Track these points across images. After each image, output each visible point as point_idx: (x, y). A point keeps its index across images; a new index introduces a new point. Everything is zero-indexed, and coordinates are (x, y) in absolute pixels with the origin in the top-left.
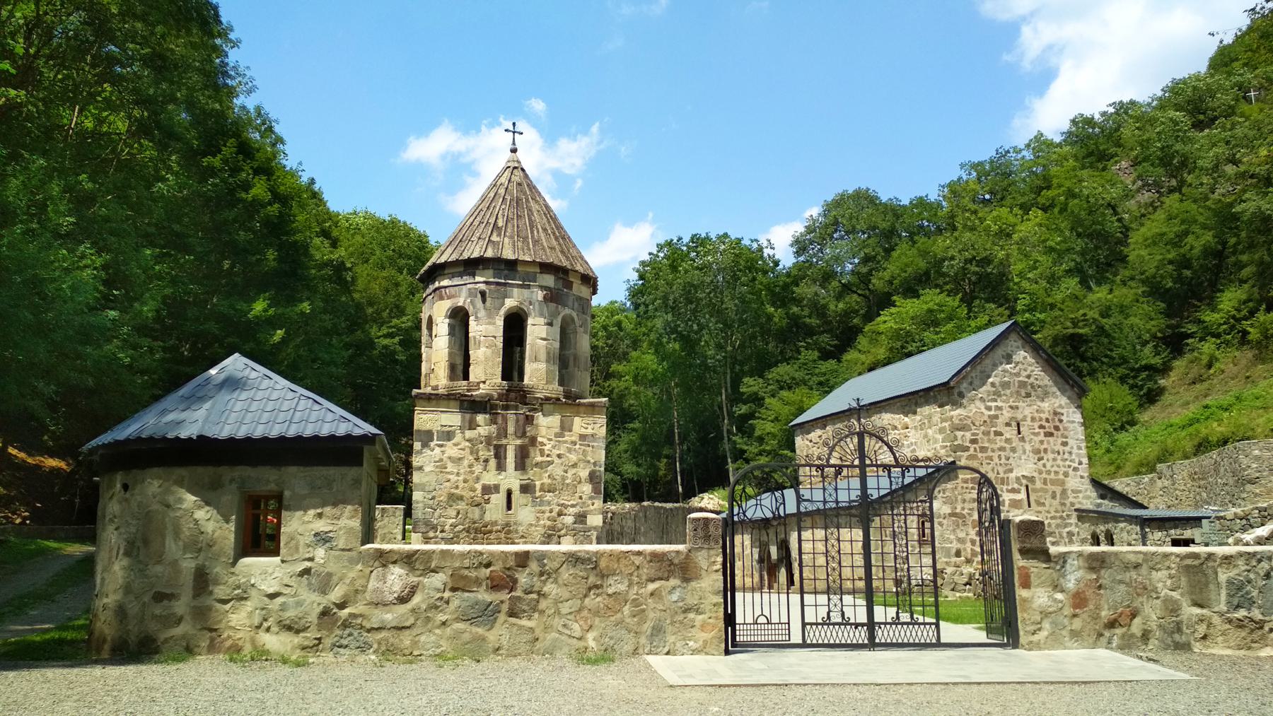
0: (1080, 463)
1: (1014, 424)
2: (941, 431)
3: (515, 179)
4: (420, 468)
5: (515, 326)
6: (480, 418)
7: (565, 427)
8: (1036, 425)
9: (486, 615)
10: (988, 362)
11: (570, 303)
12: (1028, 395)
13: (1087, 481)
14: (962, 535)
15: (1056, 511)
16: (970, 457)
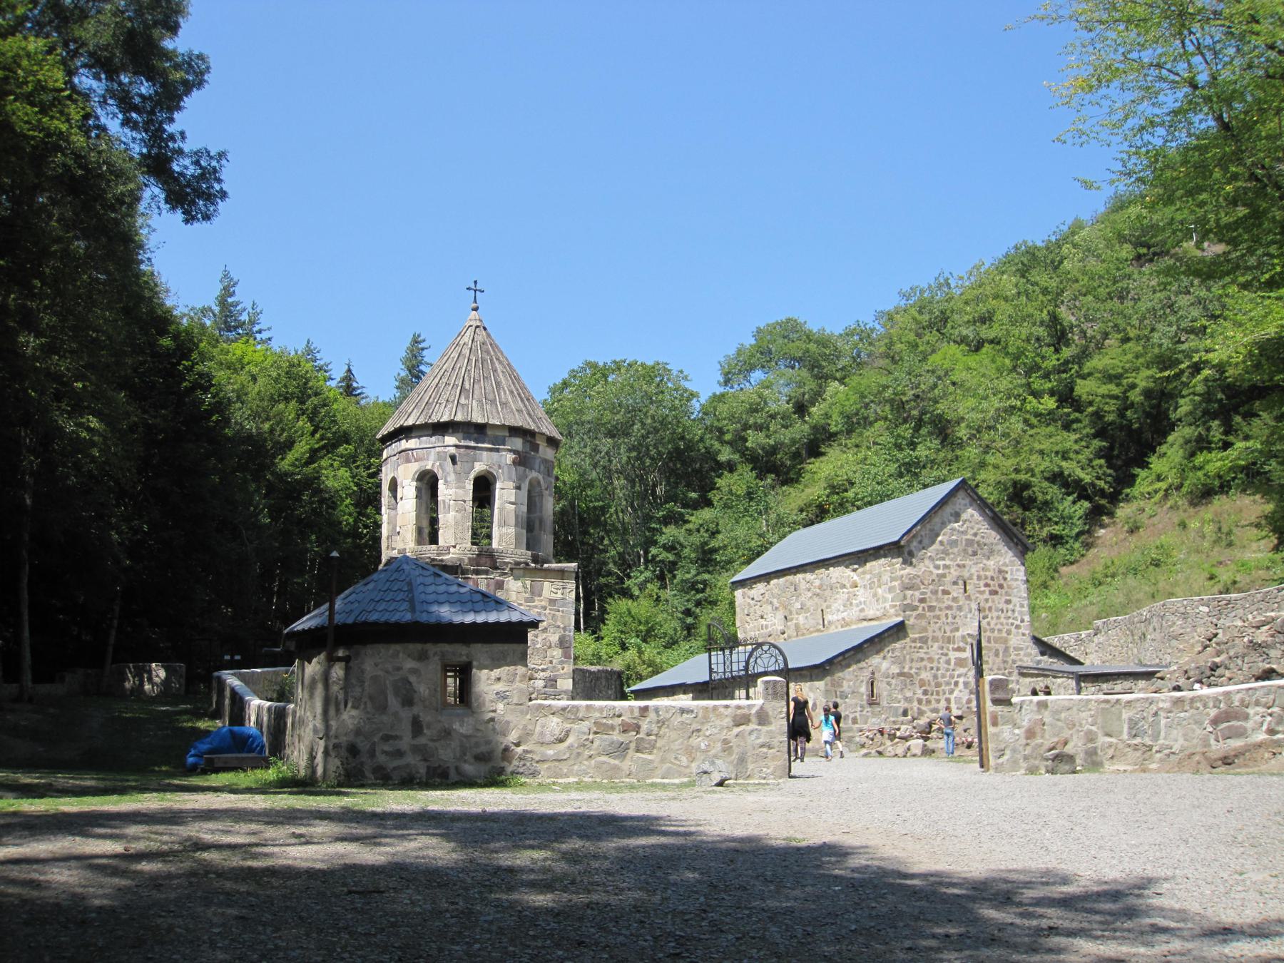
0: (1022, 621)
1: (961, 582)
2: (891, 590)
3: (479, 338)
5: (483, 489)
8: (982, 583)
9: (620, 750)
10: (937, 520)
11: (537, 467)
12: (975, 554)
13: (1028, 638)
14: (909, 694)
15: (999, 669)
16: (919, 617)
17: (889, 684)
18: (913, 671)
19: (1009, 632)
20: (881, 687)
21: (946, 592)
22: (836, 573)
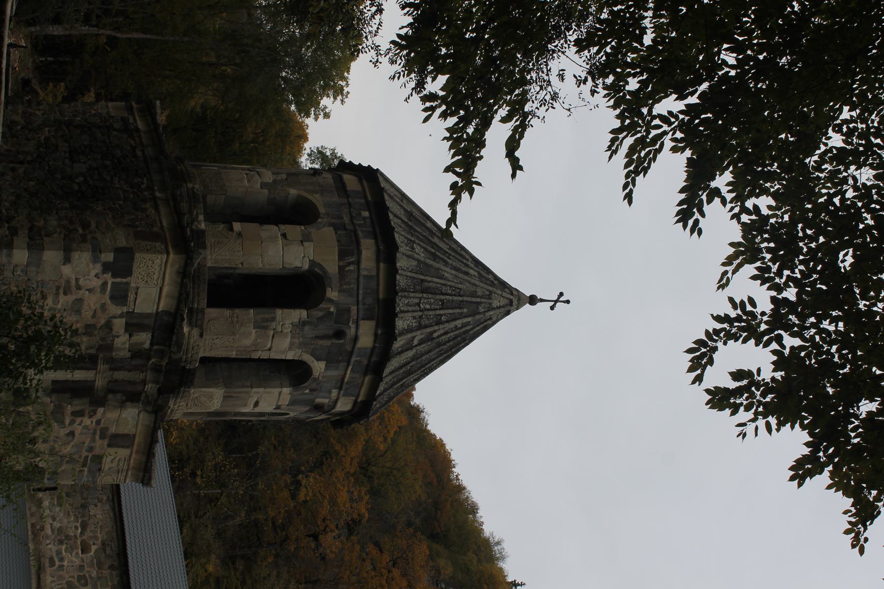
4: (67, 260)
6: (144, 338)
7: (118, 440)
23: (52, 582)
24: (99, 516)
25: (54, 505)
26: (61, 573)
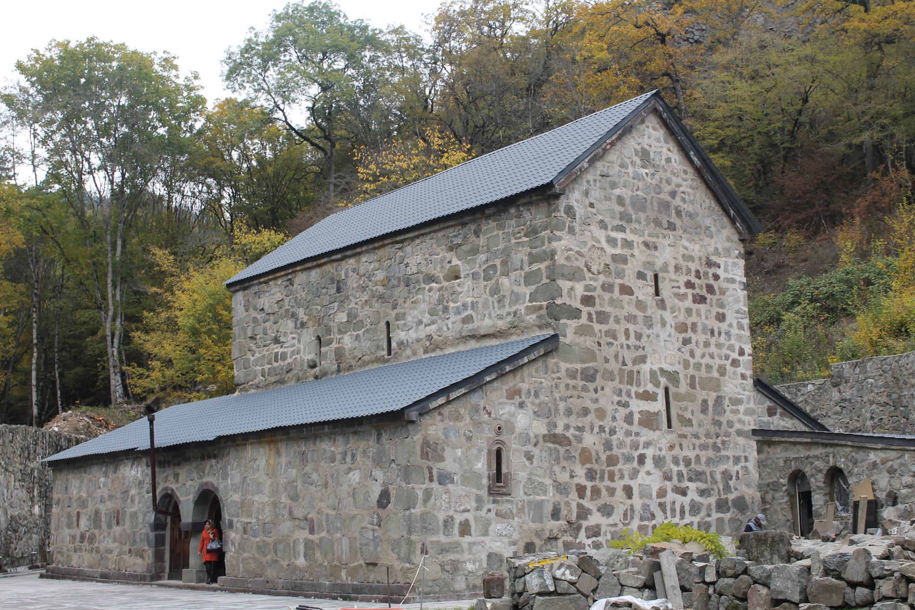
0: (742, 353)
1: (650, 275)
2: (529, 278)
8: (683, 279)
12: (672, 227)
13: (750, 382)
14: (564, 477)
15: (708, 435)
16: (582, 331)
17: (530, 457)
18: (570, 433)
19: (722, 371)
20: (515, 463)
21: (626, 290)
22: (416, 257)
23: (490, 318)
24: (419, 259)
25: (405, 324)
26: (480, 305)
